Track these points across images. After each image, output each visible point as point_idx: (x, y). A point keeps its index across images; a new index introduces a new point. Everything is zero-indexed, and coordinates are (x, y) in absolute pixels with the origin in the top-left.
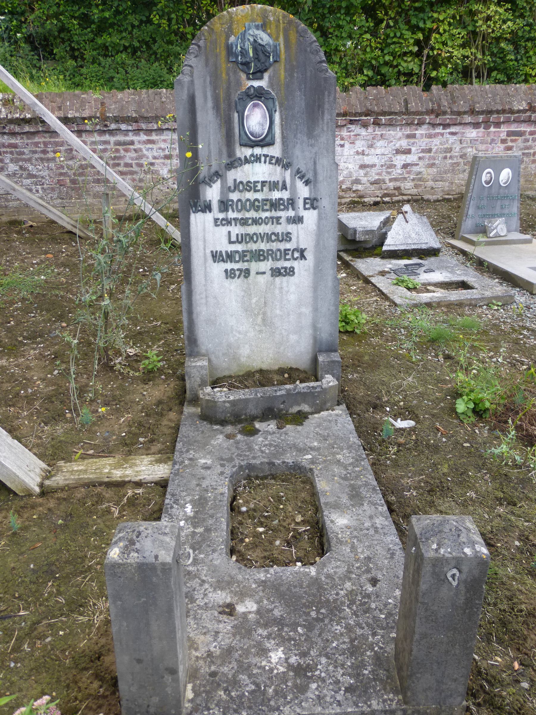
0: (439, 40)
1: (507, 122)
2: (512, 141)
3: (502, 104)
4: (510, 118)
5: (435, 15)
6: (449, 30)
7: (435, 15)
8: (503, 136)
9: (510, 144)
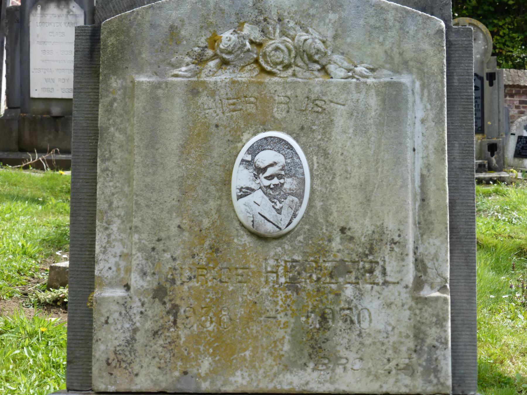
0: (500, 41)
1: (518, 94)
2: (524, 107)
3: (513, 82)
4: (519, 91)
5: (496, 21)
6: (509, 34)
7: (496, 21)
8: (517, 103)
9: (522, 109)
